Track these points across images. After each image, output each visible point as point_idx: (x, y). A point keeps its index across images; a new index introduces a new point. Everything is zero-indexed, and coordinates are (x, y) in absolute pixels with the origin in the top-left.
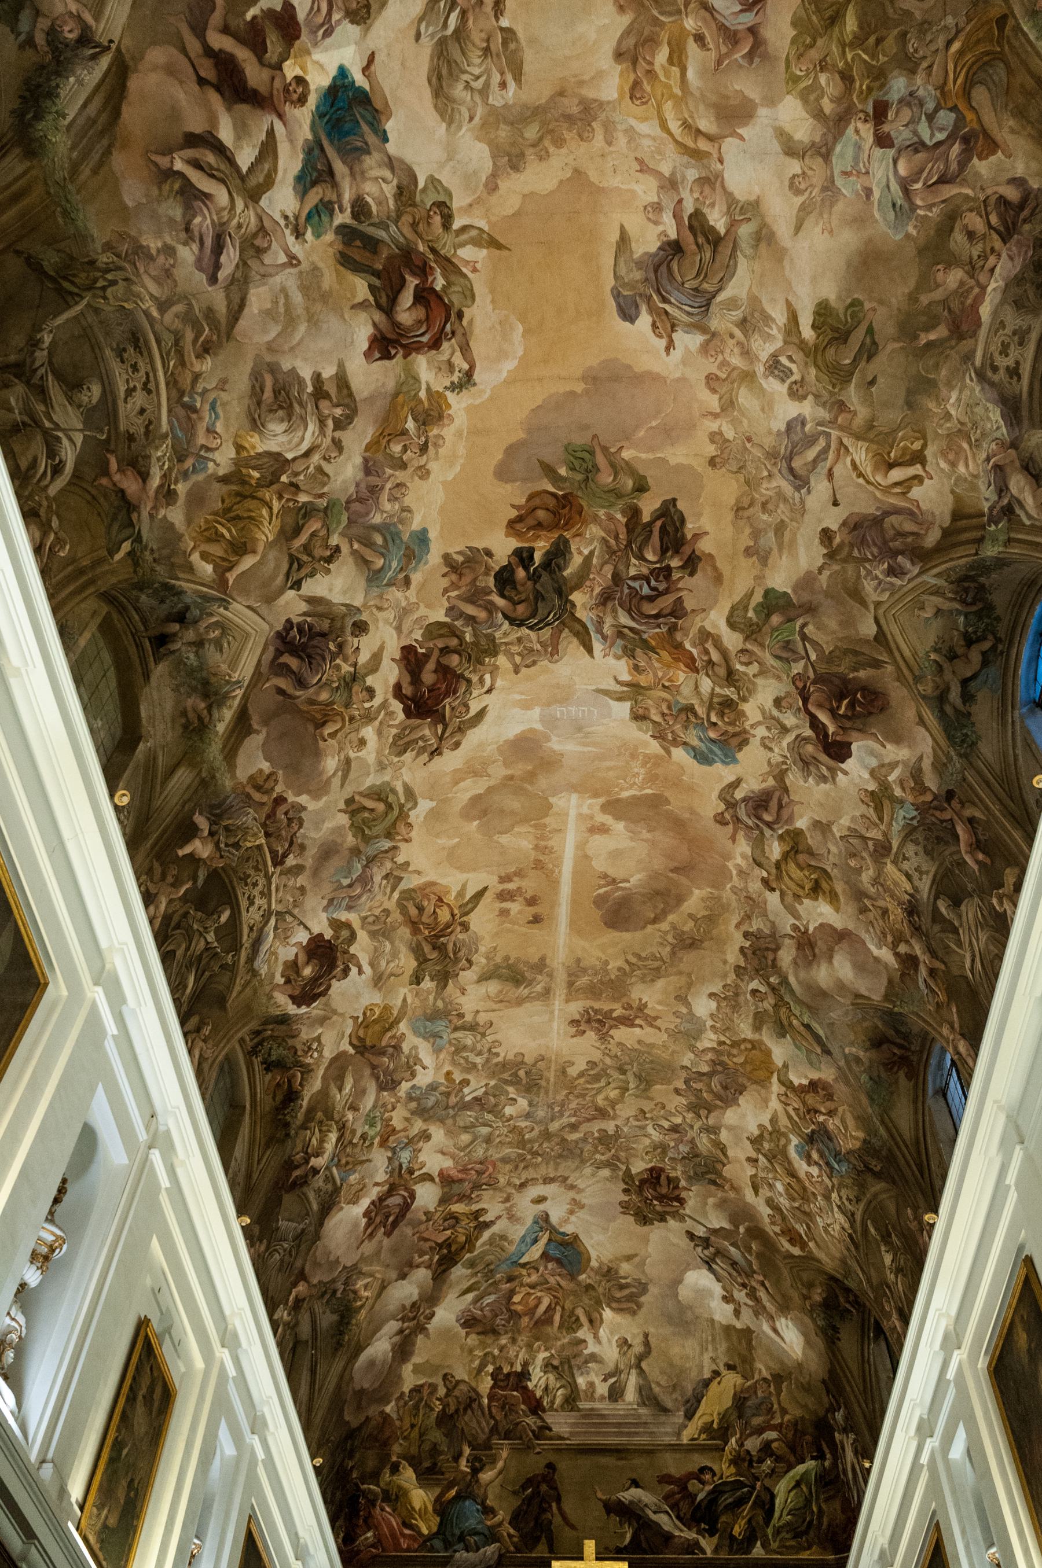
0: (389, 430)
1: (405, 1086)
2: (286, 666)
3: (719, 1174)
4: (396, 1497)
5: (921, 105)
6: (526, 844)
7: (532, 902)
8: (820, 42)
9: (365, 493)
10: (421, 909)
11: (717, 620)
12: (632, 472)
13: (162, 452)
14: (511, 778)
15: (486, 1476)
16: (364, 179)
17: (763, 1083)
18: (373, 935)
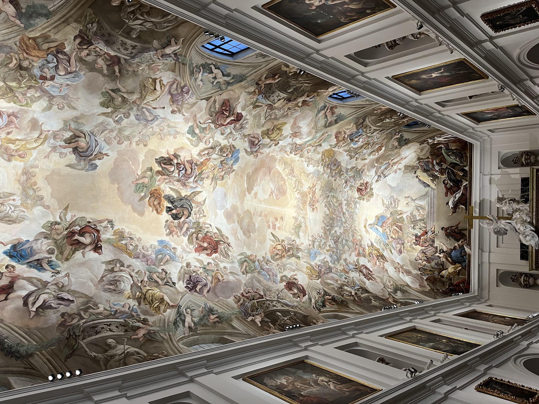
0: (125, 249)
1: (330, 264)
2: (200, 289)
3: (360, 170)
5: (44, 65)
6: (259, 218)
7: (276, 219)
8: (17, 95)
9: (145, 259)
10: (277, 254)
11: (195, 151)
12: (145, 172)
13: (130, 322)
14: (238, 221)
16: (41, 250)
17: (334, 153)
18: (284, 270)
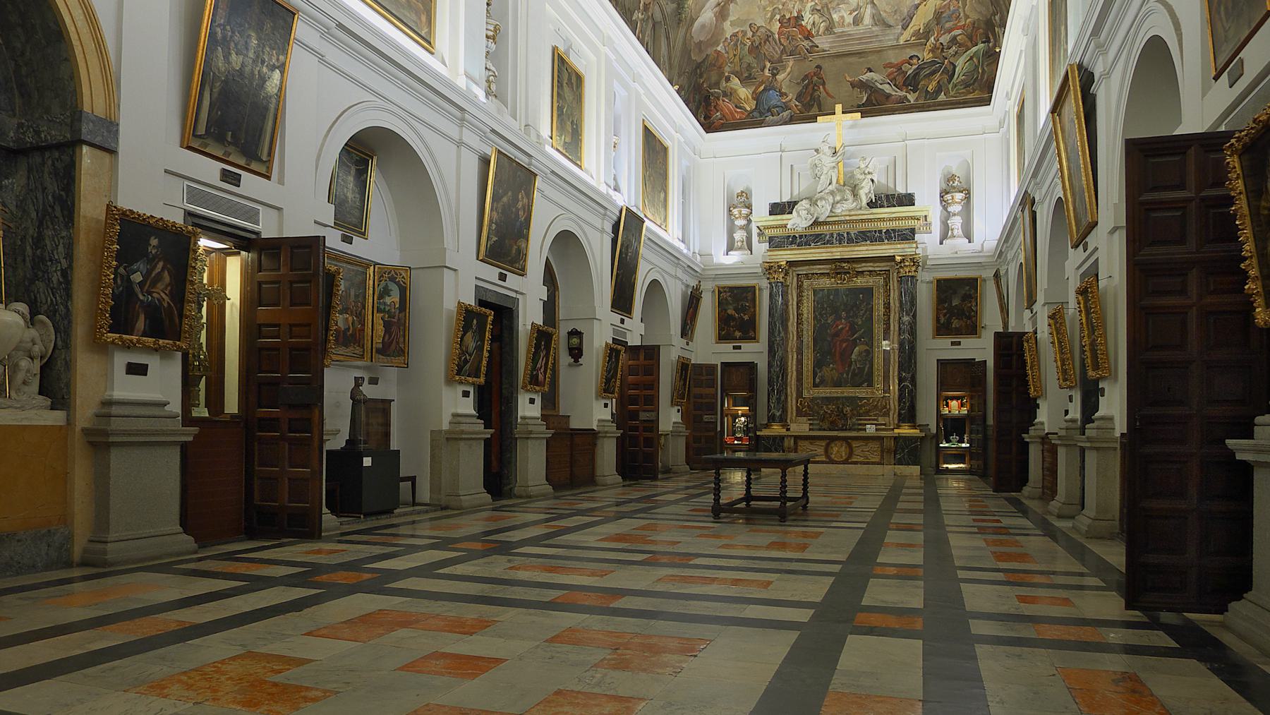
4: (729, 94)
15: (780, 77)
